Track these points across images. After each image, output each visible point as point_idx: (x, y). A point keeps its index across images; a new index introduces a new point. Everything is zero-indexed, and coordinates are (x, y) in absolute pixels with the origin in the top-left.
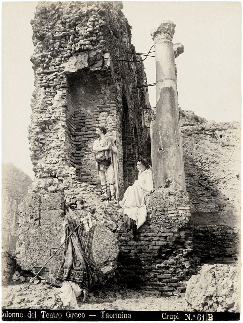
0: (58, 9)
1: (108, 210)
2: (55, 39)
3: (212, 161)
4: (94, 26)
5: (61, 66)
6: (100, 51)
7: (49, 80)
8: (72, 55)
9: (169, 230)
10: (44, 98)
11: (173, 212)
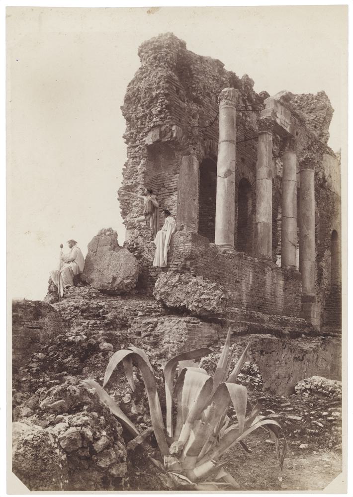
0: (137, 95)
1: (150, 249)
2: (138, 119)
4: (162, 106)
5: (143, 140)
6: (168, 125)
7: (136, 152)
8: (149, 131)
9: (179, 260)
10: (132, 167)
11: (182, 247)
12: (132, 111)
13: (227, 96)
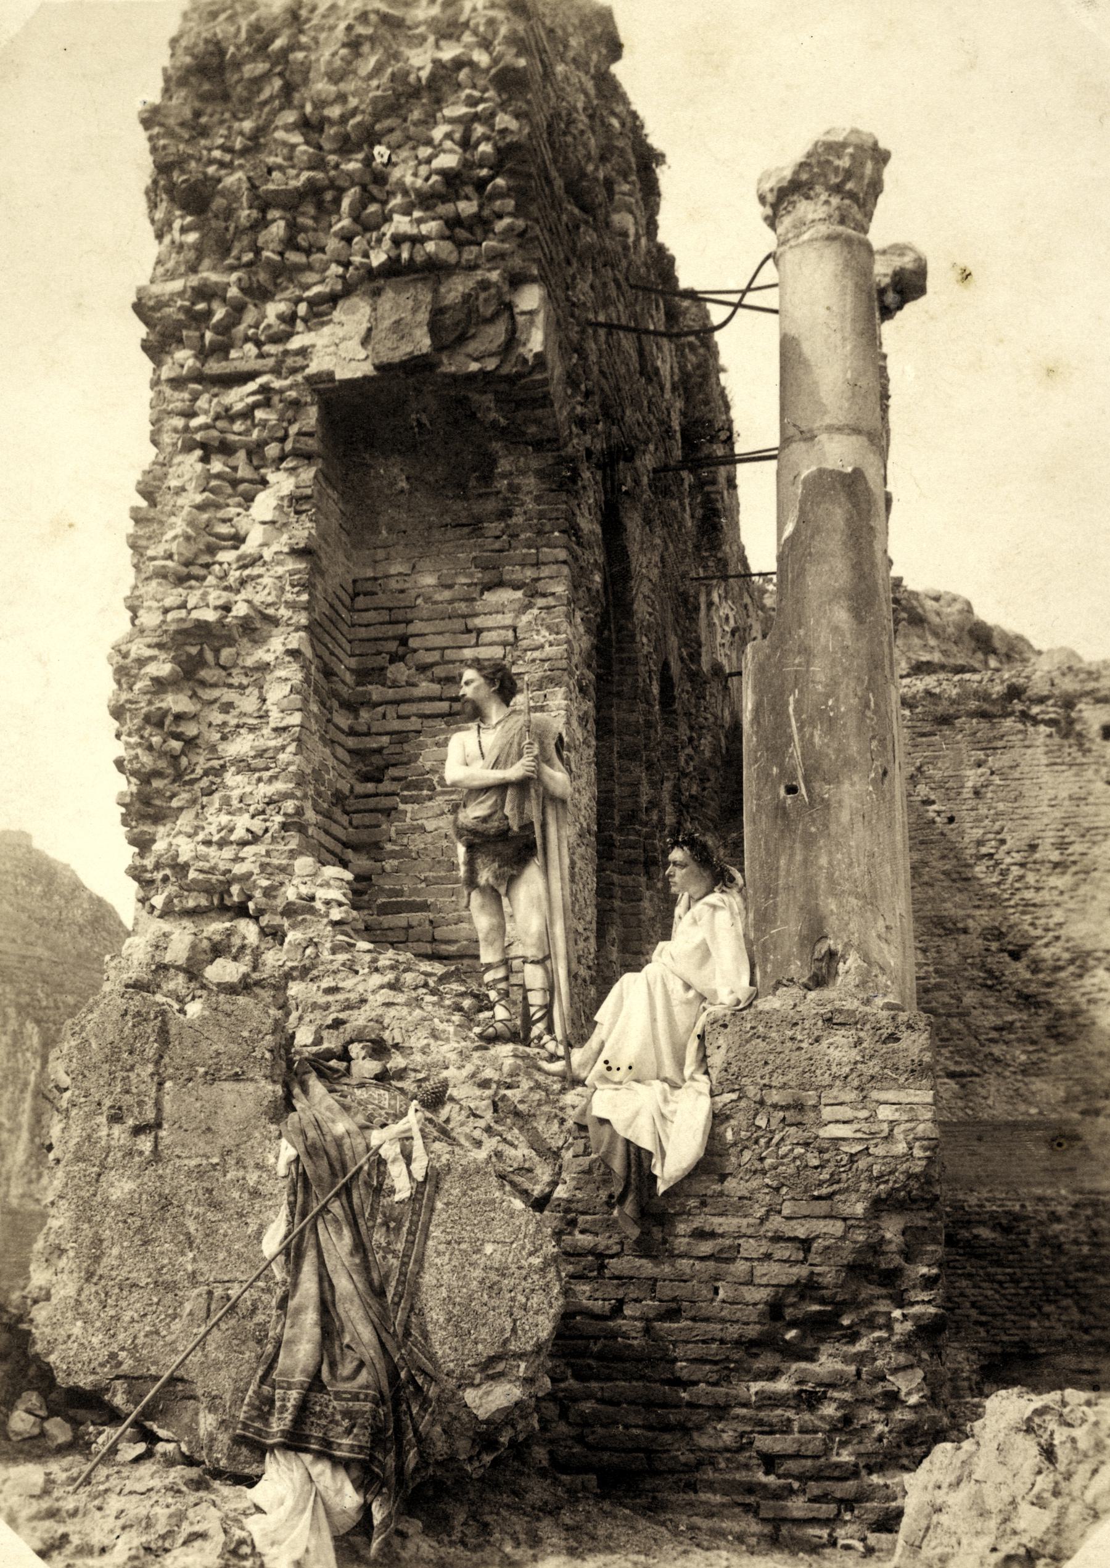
0: (286, 51)
2: (263, 204)
3: (1055, 856)
4: (466, 143)
5: (295, 343)
6: (494, 276)
7: (227, 415)
8: (348, 291)
9: (823, 1207)
10: (201, 507)
11: (846, 1112)
12: (224, 148)
13: (849, 174)
